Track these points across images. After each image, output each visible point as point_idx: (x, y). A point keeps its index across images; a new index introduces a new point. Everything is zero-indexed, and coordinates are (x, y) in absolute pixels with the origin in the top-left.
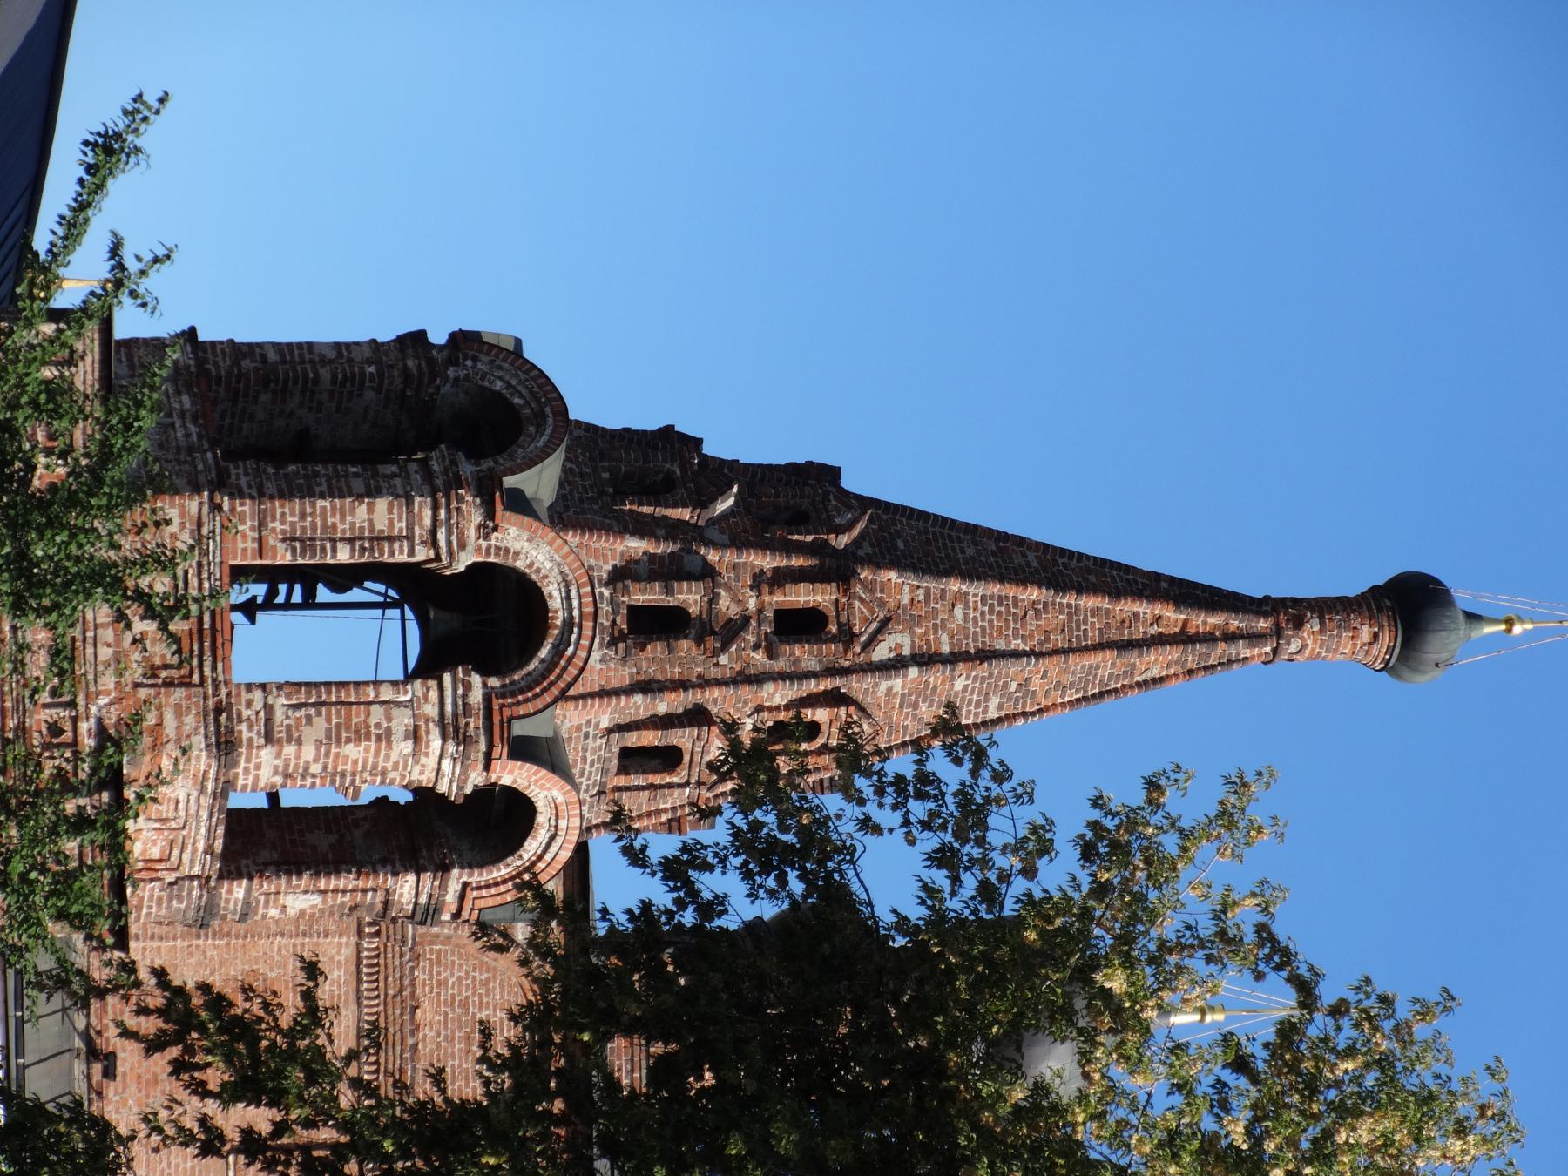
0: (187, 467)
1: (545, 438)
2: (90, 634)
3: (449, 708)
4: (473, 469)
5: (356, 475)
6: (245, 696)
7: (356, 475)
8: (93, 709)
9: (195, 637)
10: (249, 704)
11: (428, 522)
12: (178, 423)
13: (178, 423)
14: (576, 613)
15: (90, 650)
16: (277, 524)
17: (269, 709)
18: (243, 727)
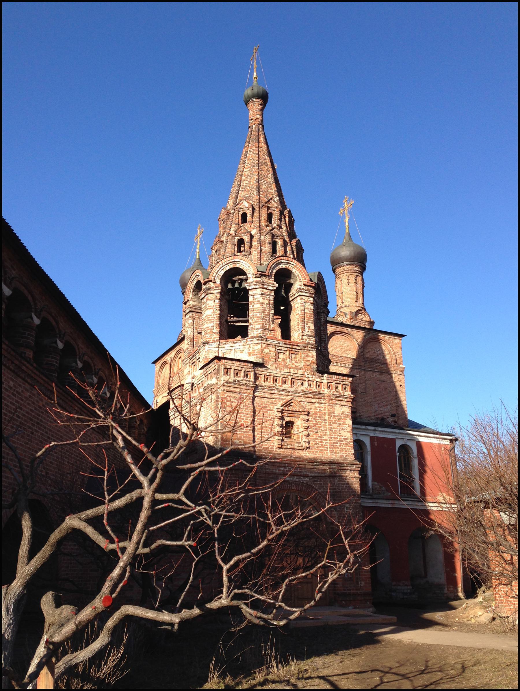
0: (251, 346)
1: (242, 261)
2: (291, 374)
3: (307, 294)
4: (251, 278)
5: (253, 306)
6: (304, 340)
7: (253, 306)
8: (307, 376)
9: (291, 349)
10: (306, 340)
11: (266, 291)
12: (234, 348)
13: (234, 348)
14: (287, 261)
15: (295, 375)
16: (268, 326)
17: (308, 335)
18: (311, 342)
